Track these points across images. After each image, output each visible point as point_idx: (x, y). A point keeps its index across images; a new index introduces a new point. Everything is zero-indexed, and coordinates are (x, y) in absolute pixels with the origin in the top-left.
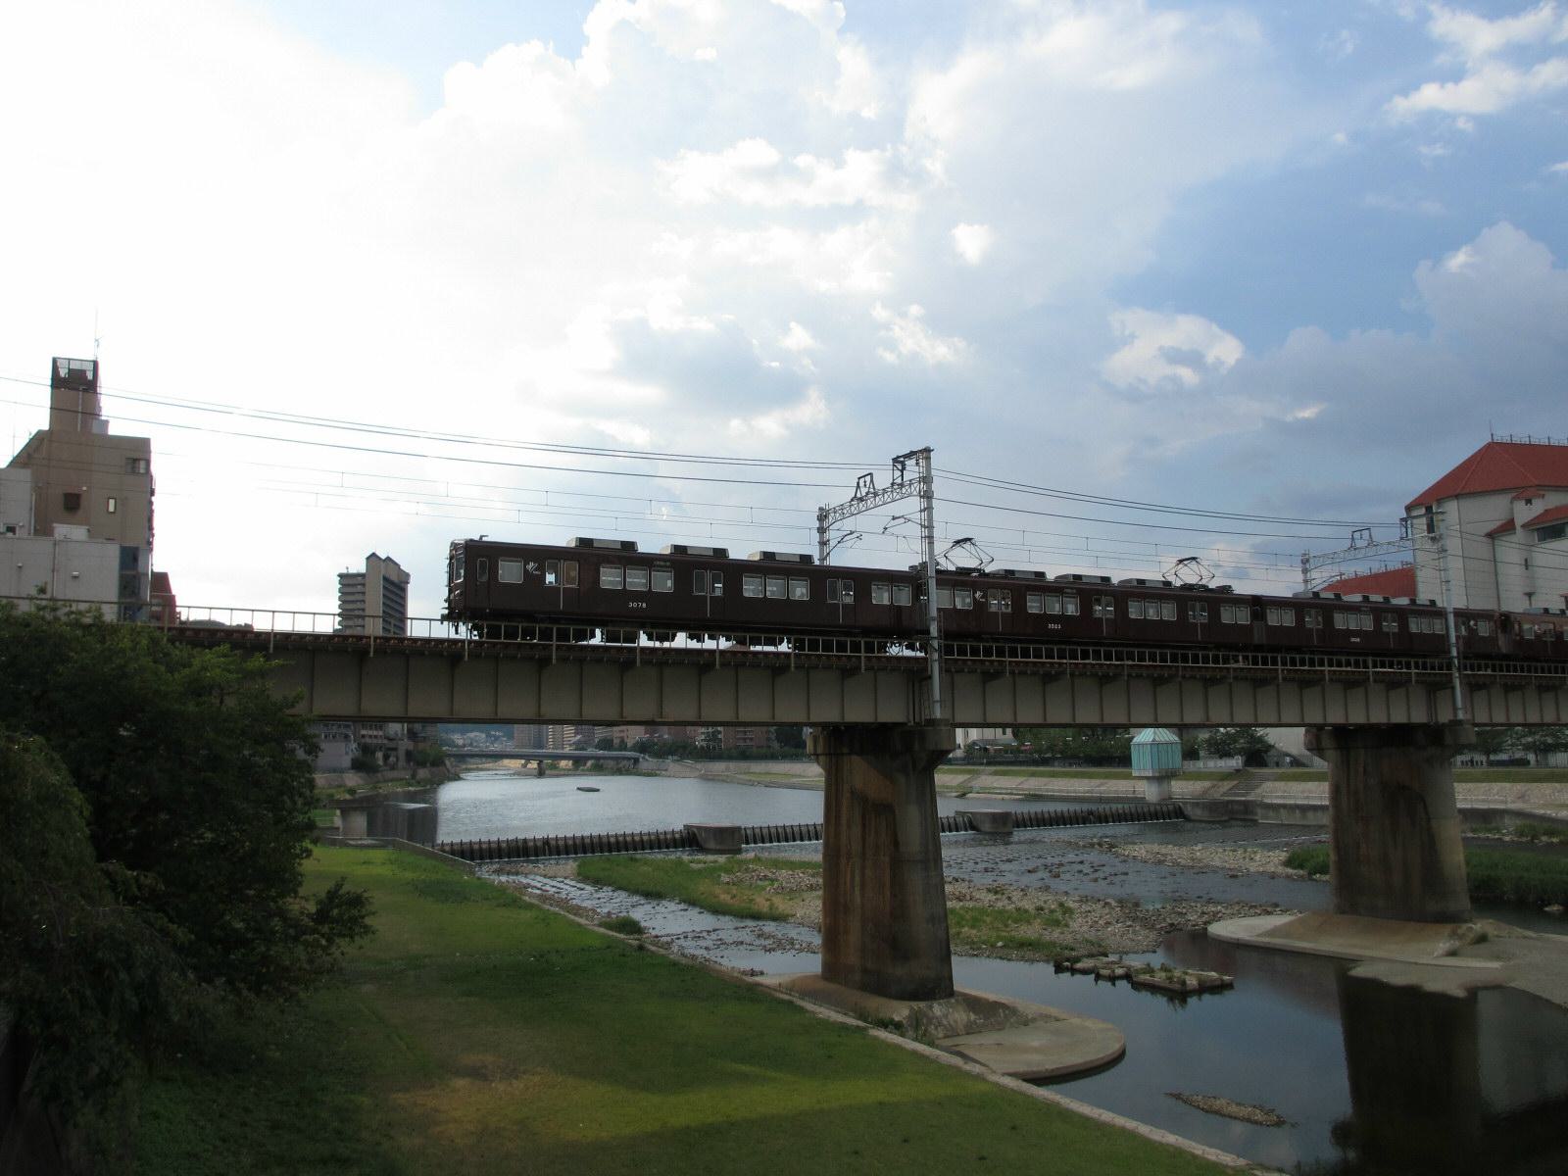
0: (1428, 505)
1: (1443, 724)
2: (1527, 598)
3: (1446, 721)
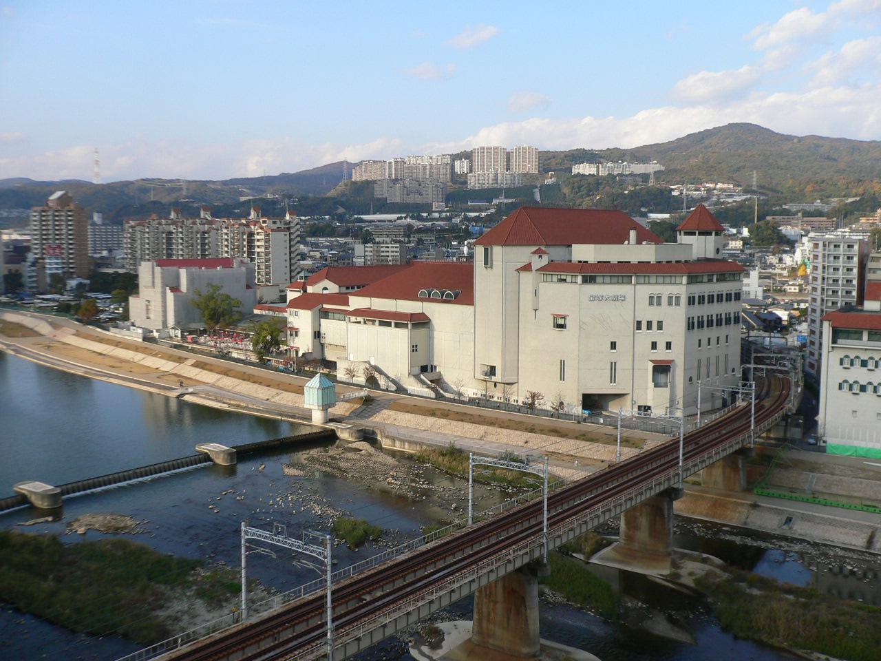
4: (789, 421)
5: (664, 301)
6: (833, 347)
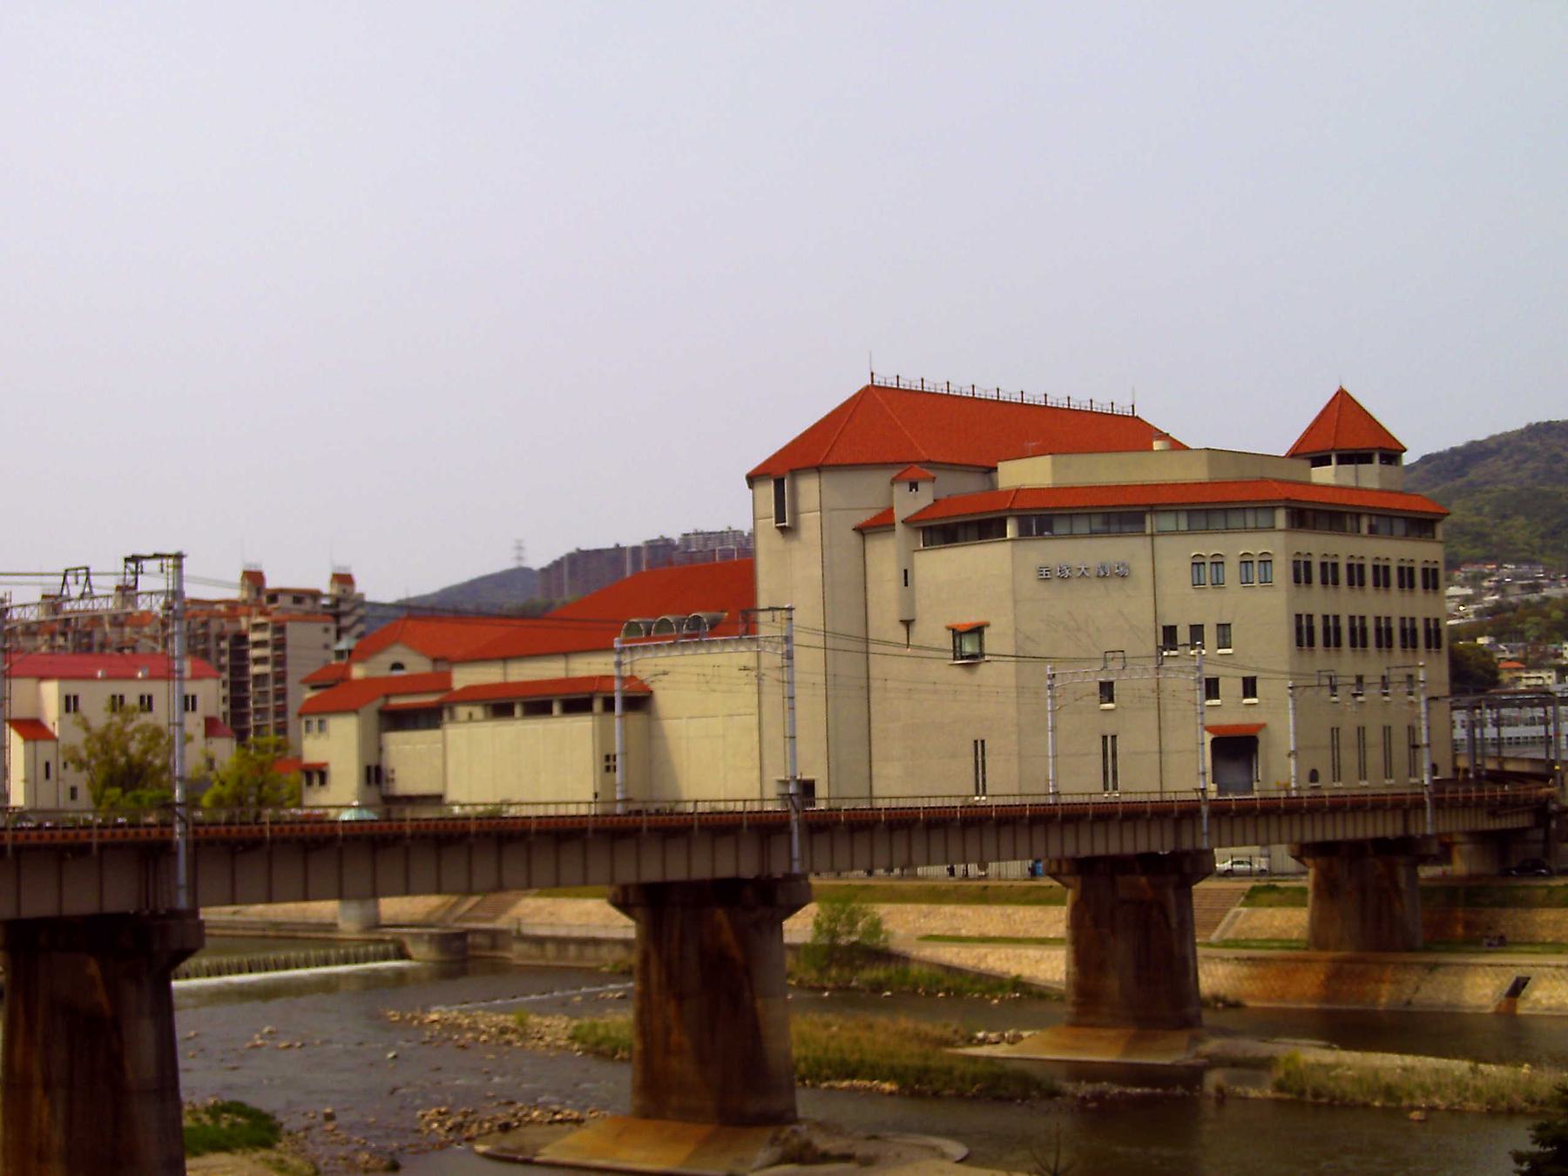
2: (903, 629)
4: (1553, 824)
5: (1232, 571)
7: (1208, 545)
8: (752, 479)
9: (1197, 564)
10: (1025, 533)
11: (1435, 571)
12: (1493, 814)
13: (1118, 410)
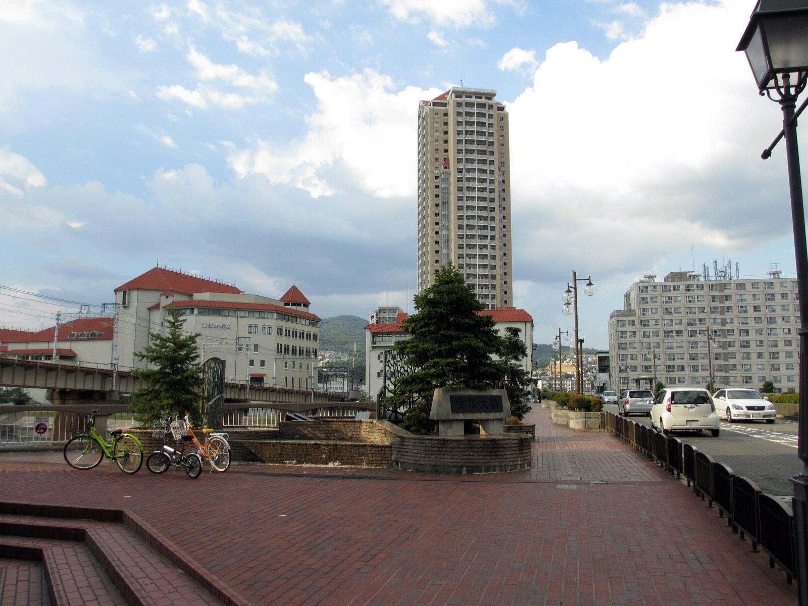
0: (125, 290)
1: (107, 391)
3: (108, 390)
6: (373, 347)
7: (253, 321)
8: (116, 291)
9: (250, 327)
10: (200, 313)
11: (316, 336)
12: (330, 400)
13: (230, 285)
